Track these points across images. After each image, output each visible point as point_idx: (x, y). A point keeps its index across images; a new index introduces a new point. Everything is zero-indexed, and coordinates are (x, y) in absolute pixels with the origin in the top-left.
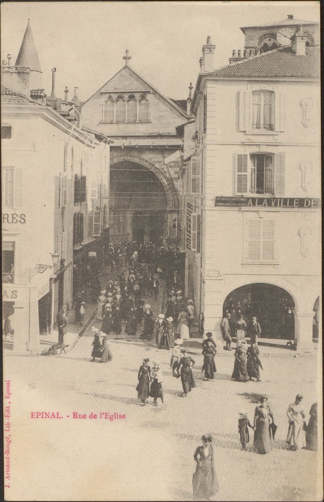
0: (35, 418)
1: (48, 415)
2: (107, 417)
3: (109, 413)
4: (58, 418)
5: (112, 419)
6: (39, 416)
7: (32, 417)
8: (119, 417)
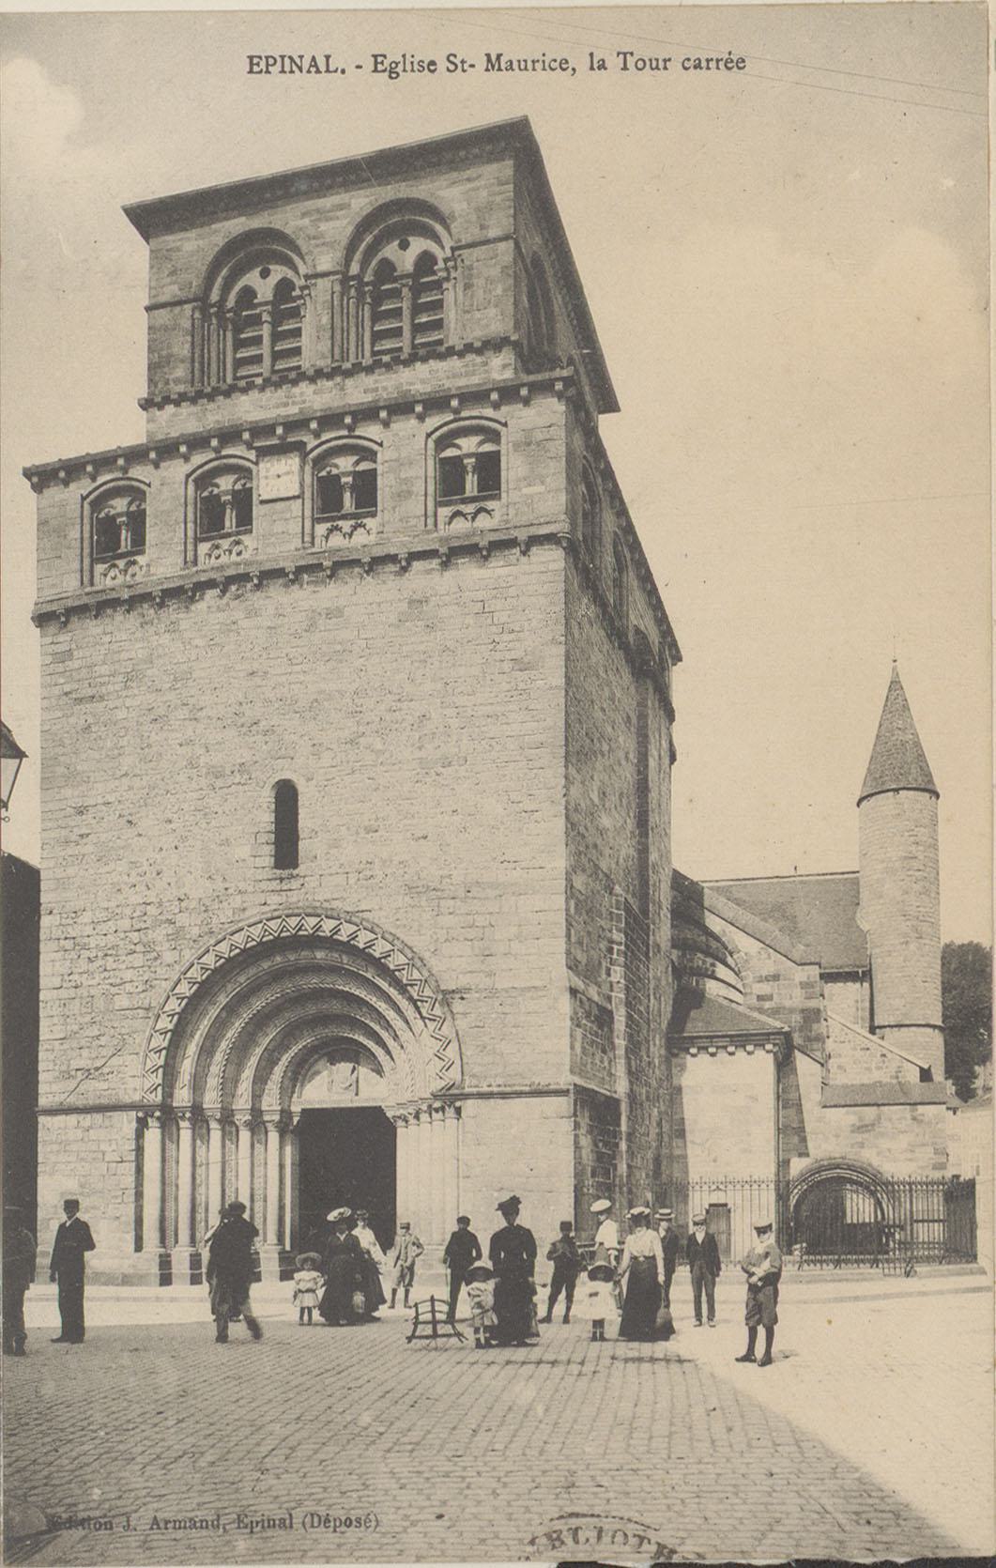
0: (261, 72)
2: (380, 67)
4: (328, 71)
5: (394, 75)
6: (270, 68)
8: (416, 67)
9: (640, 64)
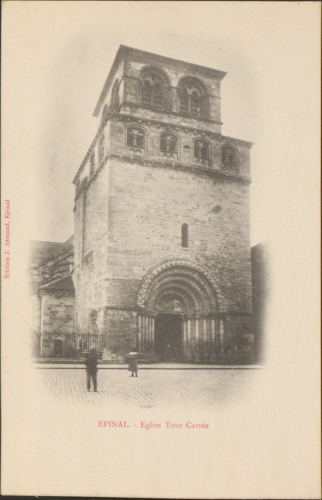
0: (102, 426)
1: (115, 423)
3: (145, 422)
4: (125, 426)
5: (148, 428)
7: (142, 427)
8: (155, 426)
9: (173, 426)
